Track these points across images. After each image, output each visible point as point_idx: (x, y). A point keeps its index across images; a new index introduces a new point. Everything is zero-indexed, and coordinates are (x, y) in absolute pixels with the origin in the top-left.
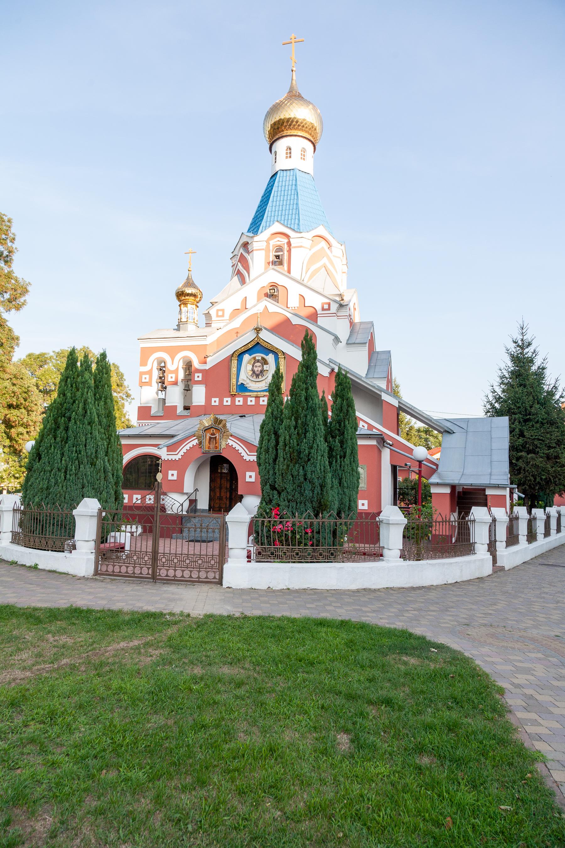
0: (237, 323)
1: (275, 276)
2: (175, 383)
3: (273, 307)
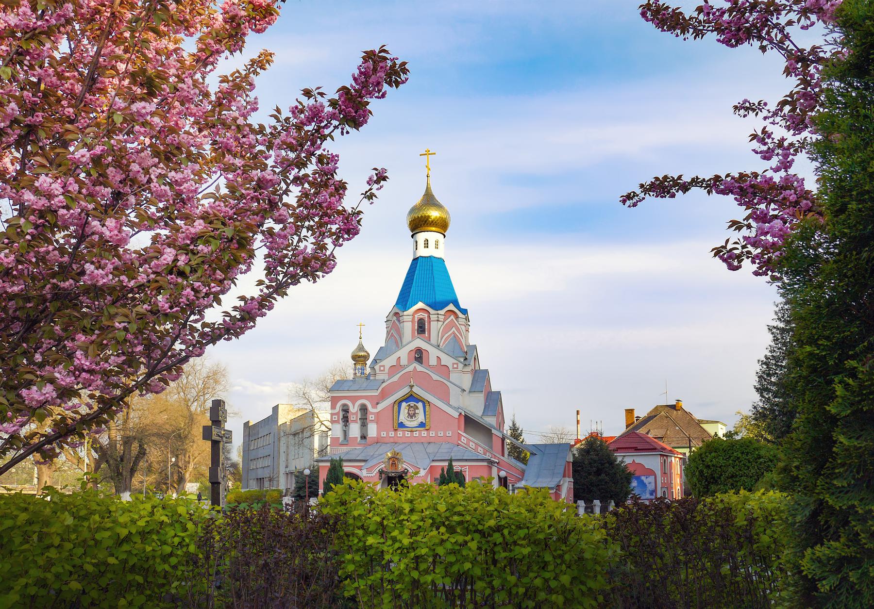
0: (395, 378)
1: (419, 343)
2: (355, 421)
3: (419, 368)
